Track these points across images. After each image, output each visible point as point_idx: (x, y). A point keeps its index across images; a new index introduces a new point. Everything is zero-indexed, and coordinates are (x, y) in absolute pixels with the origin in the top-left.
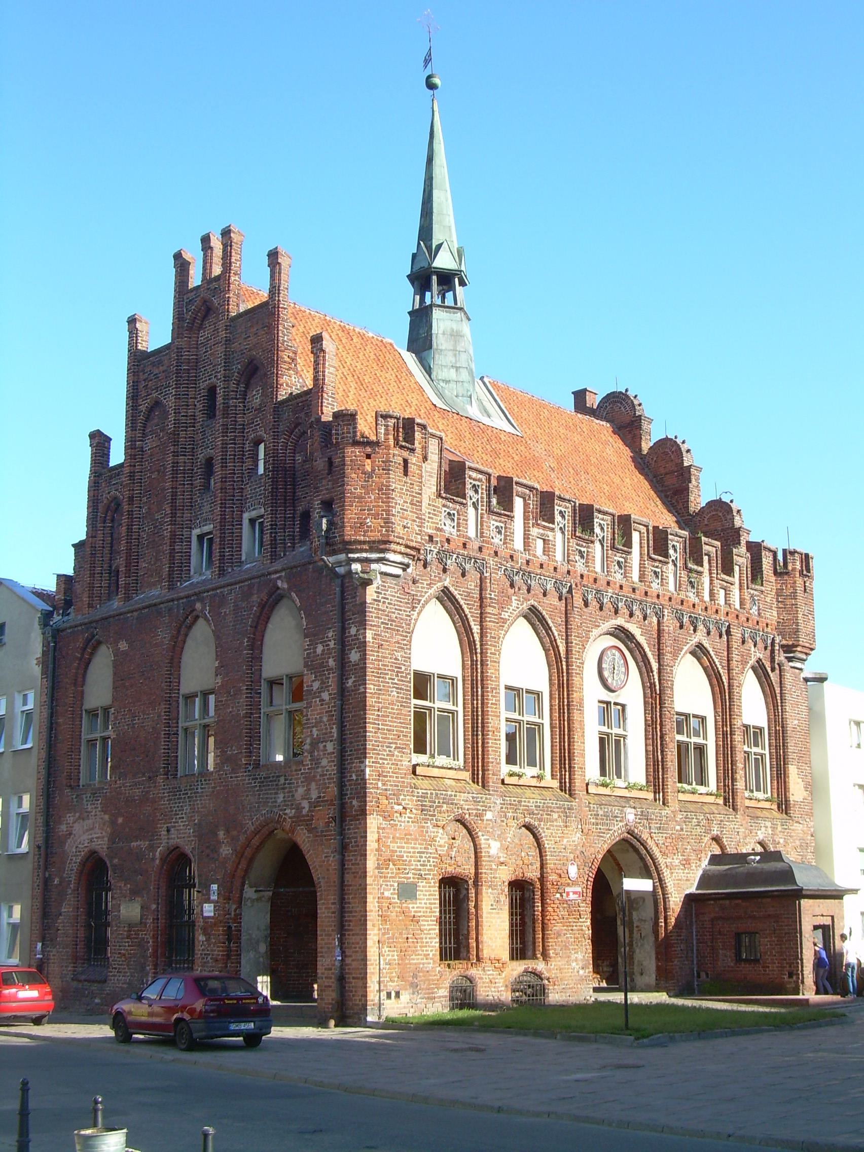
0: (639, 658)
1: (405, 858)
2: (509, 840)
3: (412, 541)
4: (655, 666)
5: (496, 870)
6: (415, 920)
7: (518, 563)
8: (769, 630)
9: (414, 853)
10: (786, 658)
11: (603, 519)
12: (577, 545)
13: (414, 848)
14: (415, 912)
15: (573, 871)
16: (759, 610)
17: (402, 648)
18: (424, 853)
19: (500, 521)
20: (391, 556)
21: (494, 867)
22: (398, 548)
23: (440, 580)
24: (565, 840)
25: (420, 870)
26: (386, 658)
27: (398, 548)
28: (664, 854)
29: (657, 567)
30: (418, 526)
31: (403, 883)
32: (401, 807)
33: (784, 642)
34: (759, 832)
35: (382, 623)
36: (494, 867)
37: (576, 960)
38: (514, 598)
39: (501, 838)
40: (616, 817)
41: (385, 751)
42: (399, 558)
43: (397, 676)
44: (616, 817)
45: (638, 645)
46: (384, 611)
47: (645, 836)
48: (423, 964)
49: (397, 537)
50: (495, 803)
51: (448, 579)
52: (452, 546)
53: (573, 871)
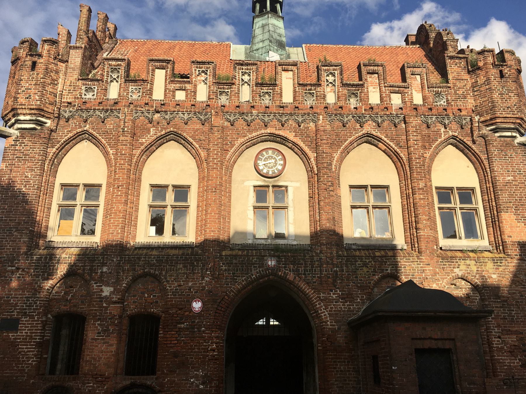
0: (300, 153)
1: (12, 301)
2: (124, 285)
3: (33, 105)
4: (312, 155)
5: (106, 308)
6: (14, 344)
7: (152, 107)
8: (464, 113)
9: (20, 298)
10: (491, 130)
11: (248, 69)
12: (219, 88)
13: (21, 294)
14: (16, 339)
15: (197, 306)
16: (447, 101)
17: (33, 170)
18: (31, 298)
19: (136, 86)
20: (22, 118)
21: (104, 305)
22: (24, 111)
23: (81, 127)
24: (190, 284)
25: (26, 309)
26: (17, 177)
27: (24, 111)
28: (317, 290)
29: (311, 90)
30: (38, 96)
31: (7, 319)
32: (14, 268)
33: (482, 119)
34: (456, 270)
35: (17, 157)
36: (104, 305)
37: (196, 377)
38: (152, 129)
39: (114, 285)
40: (254, 264)
41: (6, 233)
42: (28, 118)
43: (25, 186)
44: (254, 264)
45: (294, 144)
46: (20, 150)
47: (291, 276)
48: (17, 377)
49: (20, 105)
50: (113, 261)
51: (88, 126)
52: (88, 105)
53: (197, 306)
